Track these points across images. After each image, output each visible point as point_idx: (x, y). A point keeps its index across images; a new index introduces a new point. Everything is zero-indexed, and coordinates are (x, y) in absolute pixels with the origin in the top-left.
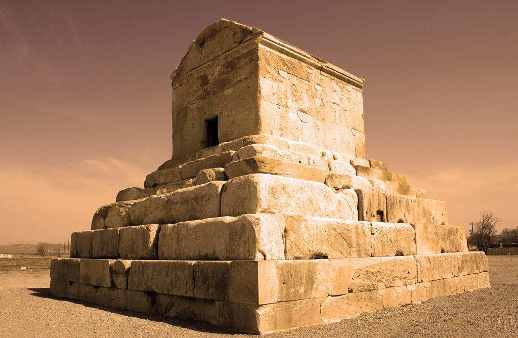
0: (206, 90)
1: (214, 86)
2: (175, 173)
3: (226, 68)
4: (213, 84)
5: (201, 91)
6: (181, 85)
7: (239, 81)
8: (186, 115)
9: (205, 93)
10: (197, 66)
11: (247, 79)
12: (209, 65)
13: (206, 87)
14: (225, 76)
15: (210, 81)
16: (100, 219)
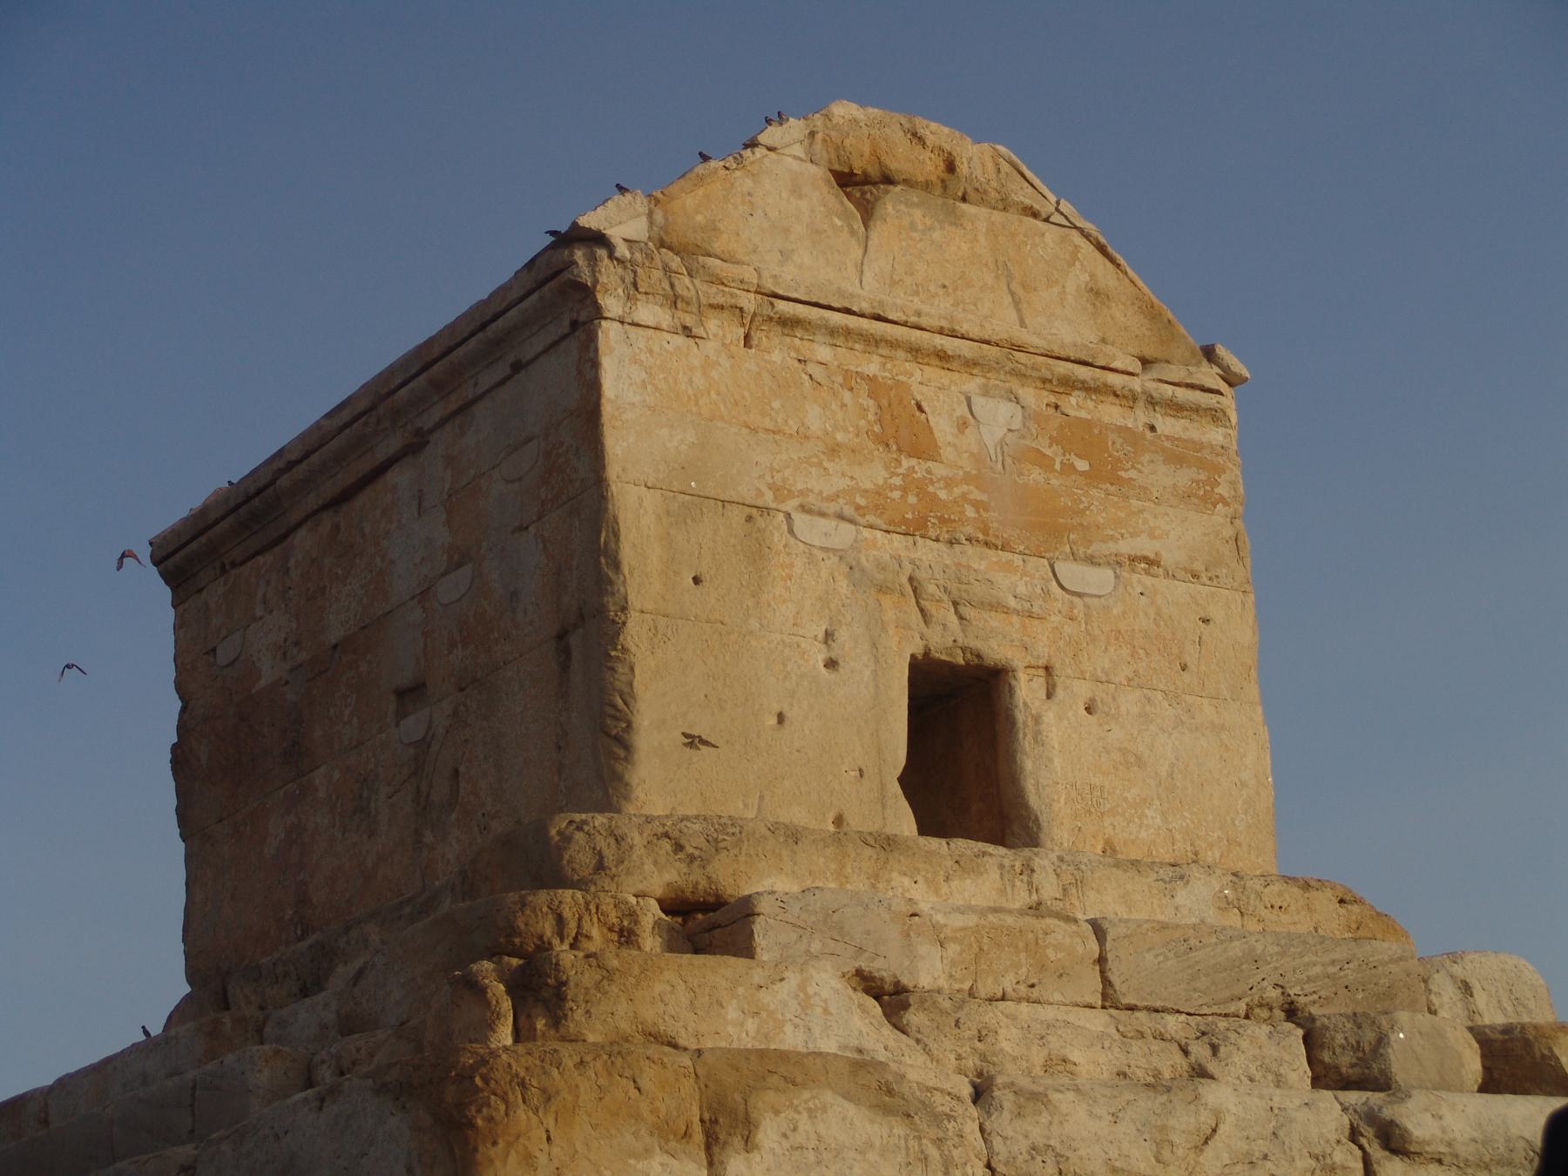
0: (920, 487)
1: (977, 495)
2: (1050, 953)
3: (1053, 441)
4: (967, 479)
5: (874, 474)
6: (687, 331)
7: (1145, 559)
8: (757, 553)
9: (912, 499)
10: (865, 307)
11: (1195, 576)
12: (942, 357)
13: (920, 468)
14: (1054, 481)
15: (947, 453)
16: (648, 1152)
